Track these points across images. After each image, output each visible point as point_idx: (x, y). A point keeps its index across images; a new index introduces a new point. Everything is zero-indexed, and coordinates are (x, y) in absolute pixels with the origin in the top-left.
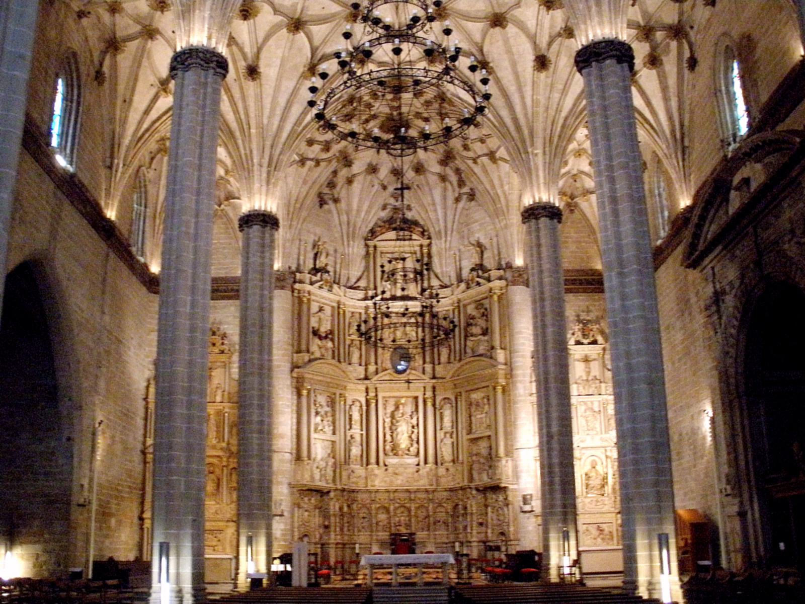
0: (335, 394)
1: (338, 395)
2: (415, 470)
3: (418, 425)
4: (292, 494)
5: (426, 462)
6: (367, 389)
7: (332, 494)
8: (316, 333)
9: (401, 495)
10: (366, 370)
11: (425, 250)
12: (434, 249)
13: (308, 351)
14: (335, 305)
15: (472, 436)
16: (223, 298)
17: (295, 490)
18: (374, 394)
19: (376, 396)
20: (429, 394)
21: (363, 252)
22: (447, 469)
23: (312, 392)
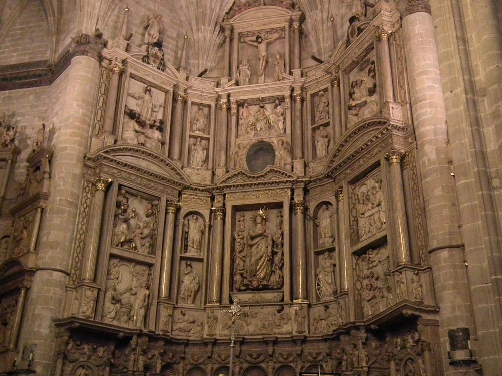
0: (159, 198)
1: (163, 203)
2: (278, 308)
3: (282, 244)
4: (58, 336)
5: (292, 296)
6: (213, 198)
7: (133, 342)
8: (132, 115)
9: (255, 349)
10: (214, 174)
11: (296, 25)
12: (308, 25)
13: (114, 131)
14: (171, 89)
15: (360, 246)
16: (21, 86)
17: (63, 329)
18: (221, 204)
19: (224, 204)
20: (298, 199)
21: (219, 41)
22: (327, 307)
23: (115, 188)
